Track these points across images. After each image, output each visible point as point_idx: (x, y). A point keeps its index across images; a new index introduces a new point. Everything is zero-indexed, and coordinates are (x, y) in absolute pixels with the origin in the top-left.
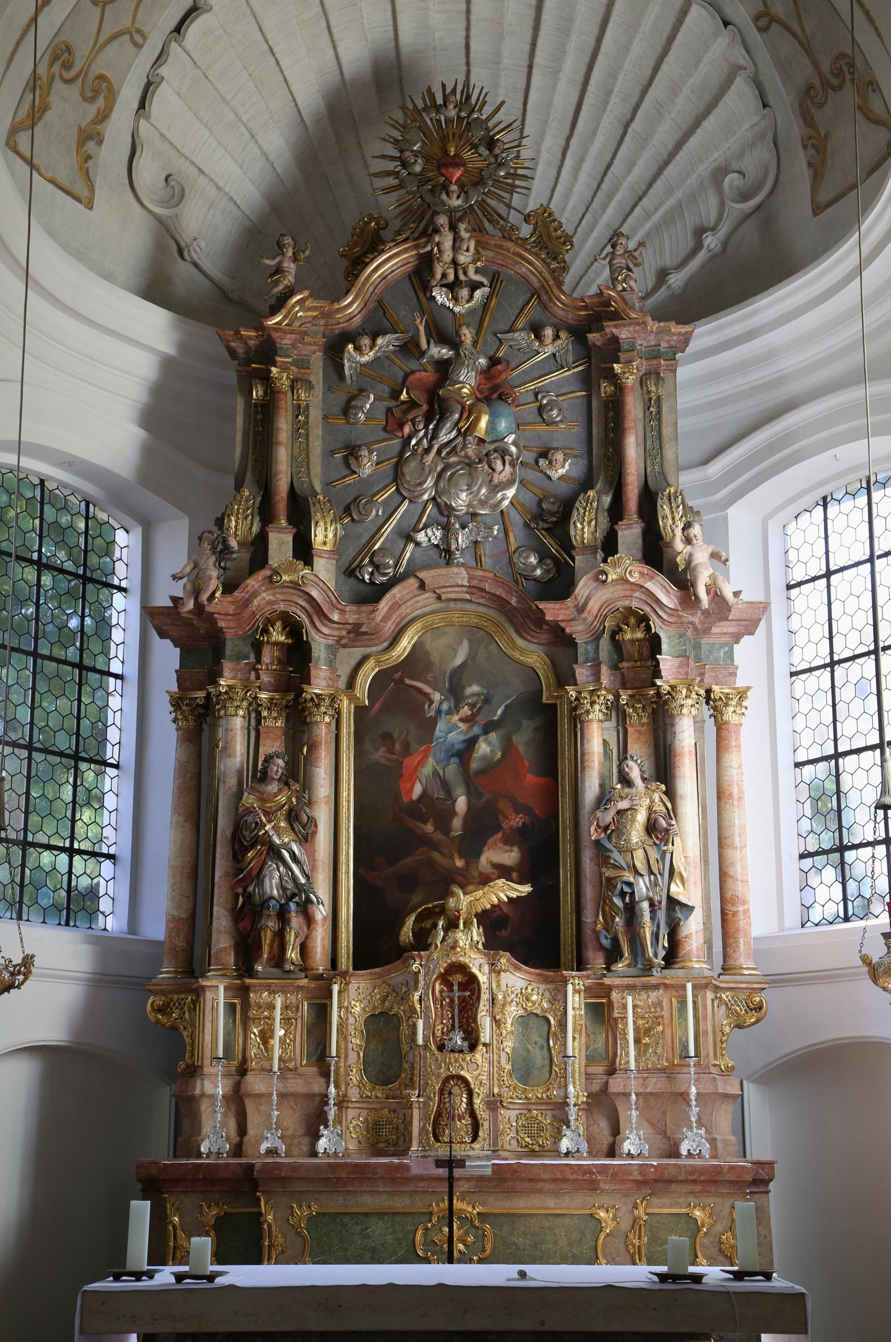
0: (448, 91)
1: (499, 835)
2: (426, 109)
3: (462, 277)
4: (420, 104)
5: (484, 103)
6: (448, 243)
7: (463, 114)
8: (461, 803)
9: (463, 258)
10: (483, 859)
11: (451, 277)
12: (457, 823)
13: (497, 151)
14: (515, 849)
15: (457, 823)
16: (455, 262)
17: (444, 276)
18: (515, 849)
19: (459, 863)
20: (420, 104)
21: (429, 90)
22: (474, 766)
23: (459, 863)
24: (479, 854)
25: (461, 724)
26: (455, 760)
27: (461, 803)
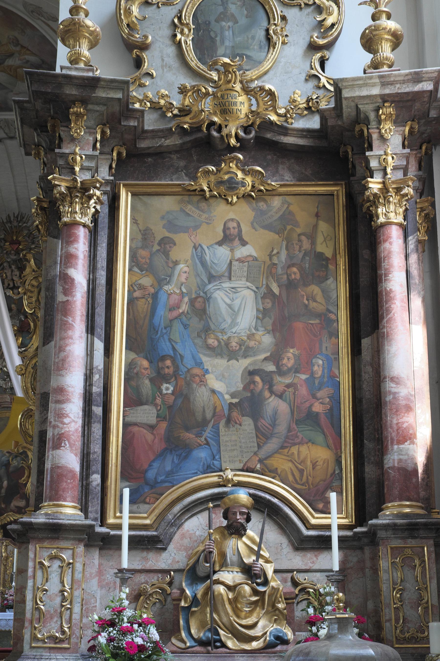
0: (16, 216)
1: (19, 495)
2: (7, 222)
3: (16, 285)
4: (5, 221)
5: (29, 220)
6: (9, 274)
7: (20, 224)
8: (5, 483)
9: (15, 278)
10: (12, 505)
11: (11, 285)
12: (3, 491)
13: (31, 238)
14: (24, 501)
15: (3, 491)
16: (13, 280)
17: (9, 285)
18: (24, 501)
19: (3, 506)
20: (5, 221)
21: (9, 215)
22: (11, 469)
23: (3, 506)
24: (11, 502)
25: (7, 454)
26: (4, 467)
27: (5, 483)
